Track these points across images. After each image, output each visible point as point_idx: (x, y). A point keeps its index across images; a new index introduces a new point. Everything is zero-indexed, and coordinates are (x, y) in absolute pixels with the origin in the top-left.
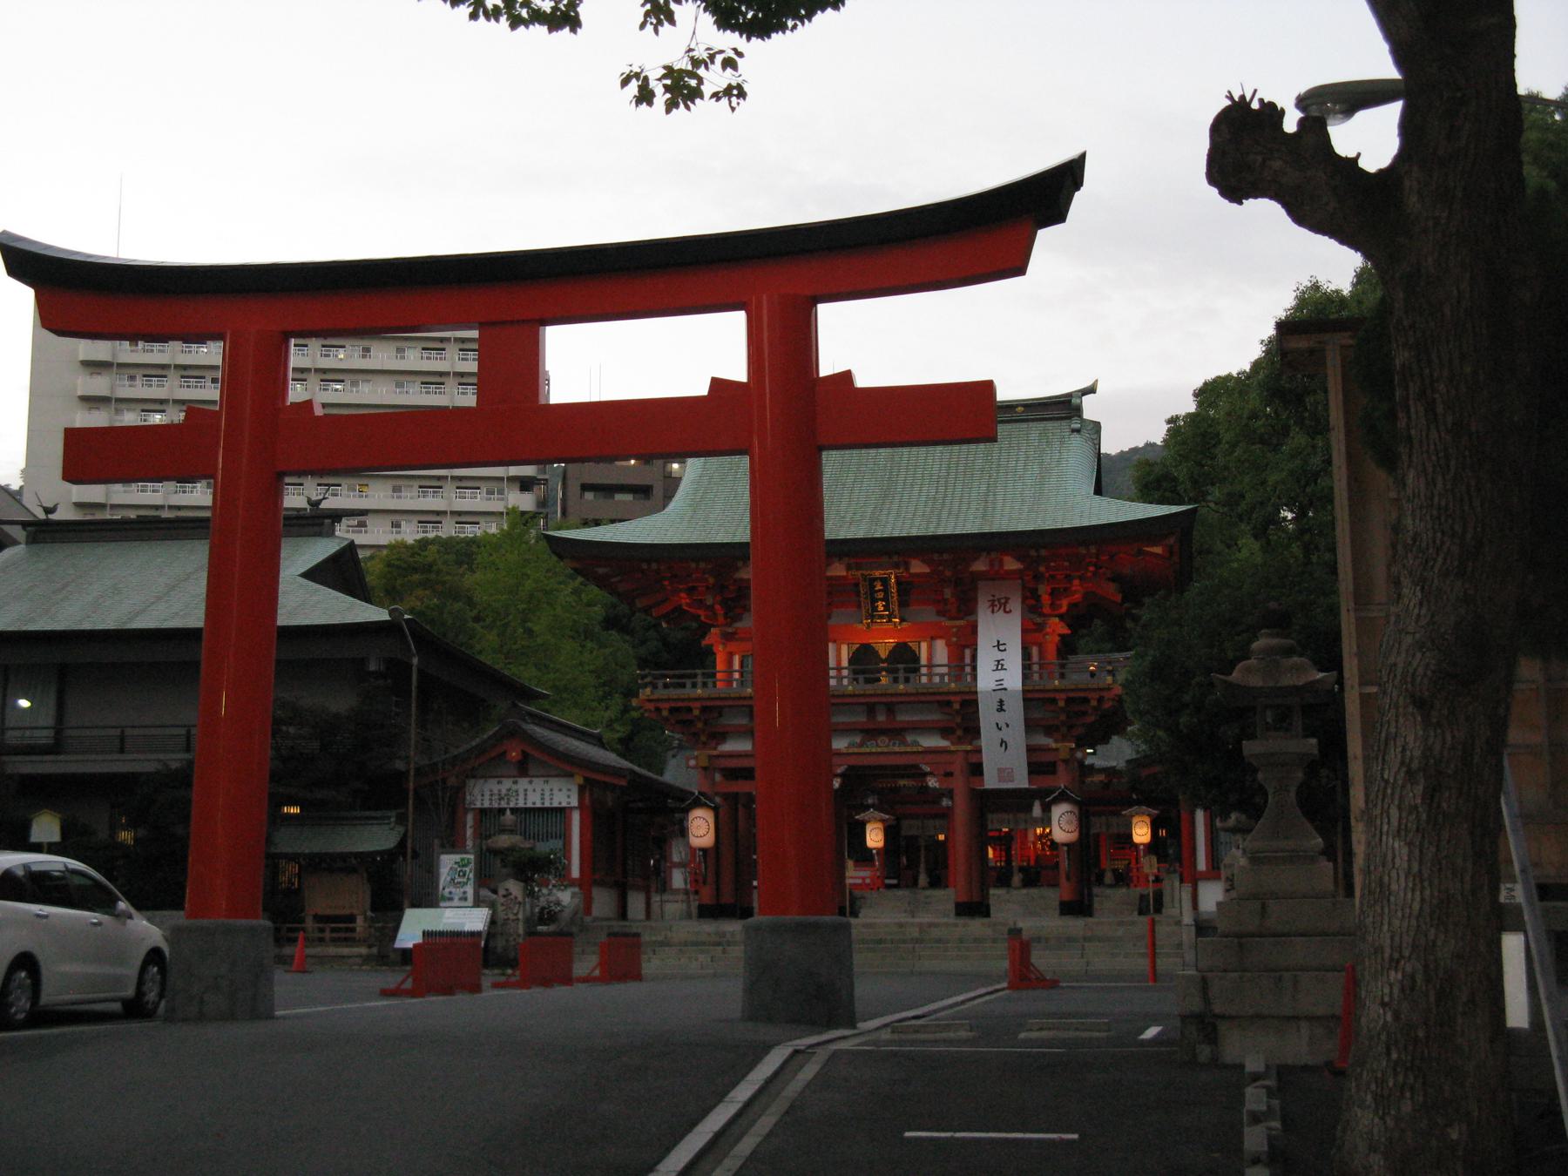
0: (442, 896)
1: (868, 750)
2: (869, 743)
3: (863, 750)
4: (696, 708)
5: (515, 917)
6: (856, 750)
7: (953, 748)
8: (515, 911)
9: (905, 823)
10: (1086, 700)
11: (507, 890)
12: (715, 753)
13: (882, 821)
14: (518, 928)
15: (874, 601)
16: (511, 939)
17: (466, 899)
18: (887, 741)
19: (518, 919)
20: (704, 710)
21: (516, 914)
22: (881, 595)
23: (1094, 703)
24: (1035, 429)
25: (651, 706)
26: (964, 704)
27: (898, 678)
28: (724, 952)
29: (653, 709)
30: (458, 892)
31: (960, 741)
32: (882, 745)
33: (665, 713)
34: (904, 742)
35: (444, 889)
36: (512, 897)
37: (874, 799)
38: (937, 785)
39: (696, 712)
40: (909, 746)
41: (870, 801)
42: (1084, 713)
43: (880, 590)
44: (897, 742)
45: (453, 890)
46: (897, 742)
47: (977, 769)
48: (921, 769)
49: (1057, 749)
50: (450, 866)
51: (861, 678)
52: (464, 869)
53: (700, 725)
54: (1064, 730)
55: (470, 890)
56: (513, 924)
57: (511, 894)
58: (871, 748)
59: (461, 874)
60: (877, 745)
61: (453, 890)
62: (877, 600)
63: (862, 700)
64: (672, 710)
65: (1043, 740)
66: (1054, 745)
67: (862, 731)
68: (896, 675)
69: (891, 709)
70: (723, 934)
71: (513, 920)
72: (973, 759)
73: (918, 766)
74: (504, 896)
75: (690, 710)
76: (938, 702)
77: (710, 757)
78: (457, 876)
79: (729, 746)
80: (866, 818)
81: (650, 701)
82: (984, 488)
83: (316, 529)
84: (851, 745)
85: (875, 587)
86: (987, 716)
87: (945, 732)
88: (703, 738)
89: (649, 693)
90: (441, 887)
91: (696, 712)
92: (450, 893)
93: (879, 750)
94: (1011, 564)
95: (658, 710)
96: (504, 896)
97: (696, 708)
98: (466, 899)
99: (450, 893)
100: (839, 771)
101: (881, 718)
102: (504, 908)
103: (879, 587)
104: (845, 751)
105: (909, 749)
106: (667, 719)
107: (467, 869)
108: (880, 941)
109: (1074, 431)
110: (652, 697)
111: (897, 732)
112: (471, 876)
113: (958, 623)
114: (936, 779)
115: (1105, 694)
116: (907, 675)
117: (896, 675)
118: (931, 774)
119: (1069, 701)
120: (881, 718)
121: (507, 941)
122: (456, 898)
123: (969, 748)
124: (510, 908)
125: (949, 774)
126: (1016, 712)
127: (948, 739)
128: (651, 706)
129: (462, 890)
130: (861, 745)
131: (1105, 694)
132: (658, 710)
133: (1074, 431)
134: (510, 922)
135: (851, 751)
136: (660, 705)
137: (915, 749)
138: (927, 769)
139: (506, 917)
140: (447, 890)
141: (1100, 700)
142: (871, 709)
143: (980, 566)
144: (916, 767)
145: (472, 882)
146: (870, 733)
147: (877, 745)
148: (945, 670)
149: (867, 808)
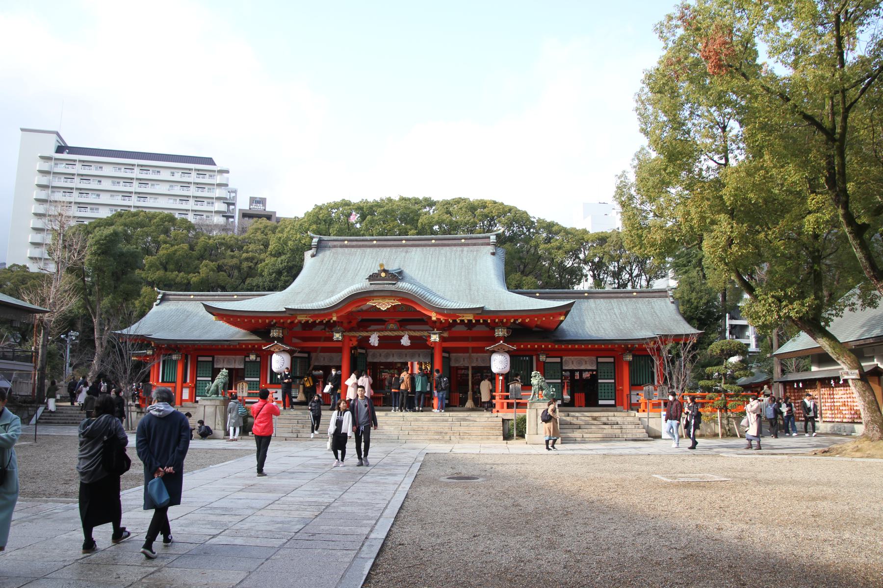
9: (313, 355)
13: (290, 352)
37: (279, 333)
80: (272, 349)
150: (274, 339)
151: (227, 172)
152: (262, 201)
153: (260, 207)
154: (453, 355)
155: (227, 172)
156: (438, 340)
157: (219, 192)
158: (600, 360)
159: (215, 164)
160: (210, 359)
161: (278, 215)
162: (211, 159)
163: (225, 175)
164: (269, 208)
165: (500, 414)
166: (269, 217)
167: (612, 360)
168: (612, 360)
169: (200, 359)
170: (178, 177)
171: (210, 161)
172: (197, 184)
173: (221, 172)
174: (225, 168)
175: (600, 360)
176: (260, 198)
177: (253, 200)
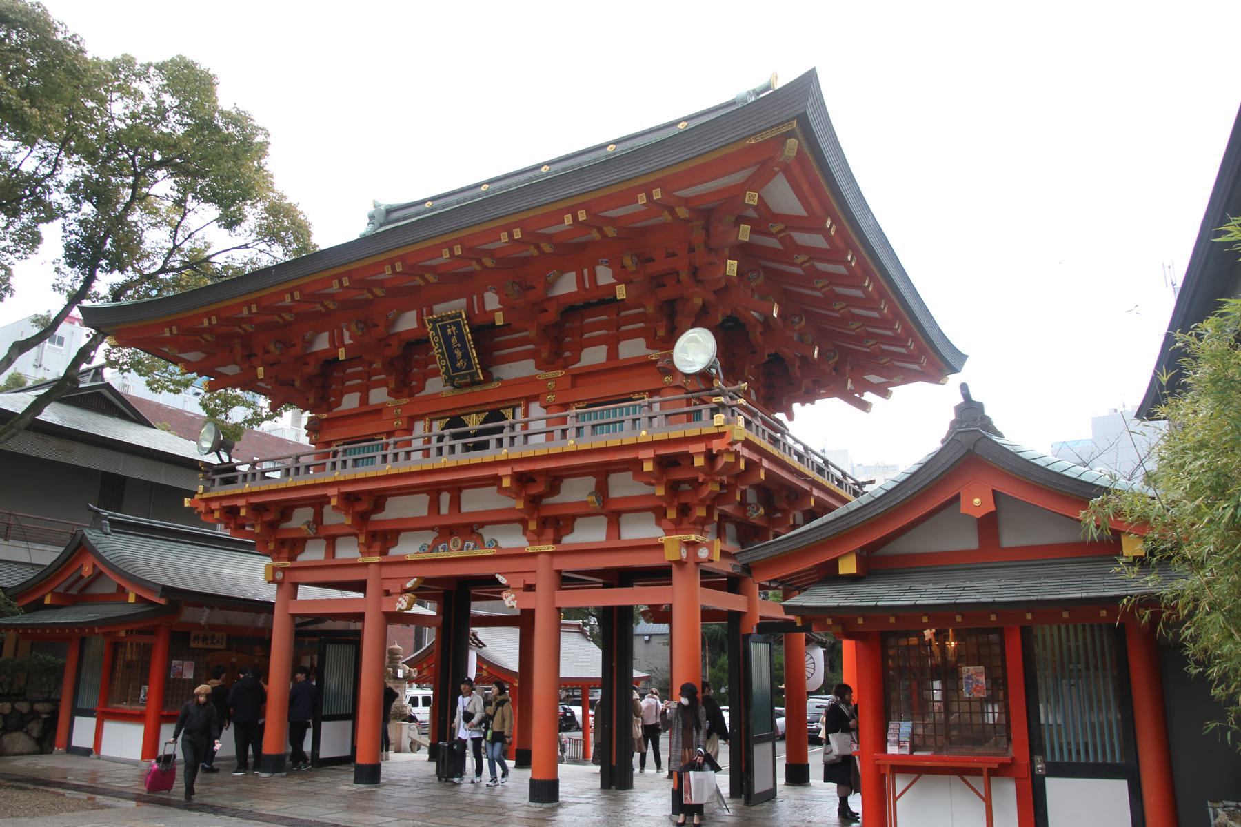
18: (460, 544)
32: (453, 549)
34: (480, 543)
38: (514, 604)
39: (243, 513)
46: (472, 545)
48: (497, 581)
67: (432, 529)
73: (494, 576)
84: (422, 549)
100: (409, 585)
111: (470, 529)
113: (559, 373)
114: (513, 596)
116: (452, 443)
125: (530, 588)
130: (433, 548)
131: (717, 445)
141: (711, 457)
146: (447, 532)
147: (450, 550)
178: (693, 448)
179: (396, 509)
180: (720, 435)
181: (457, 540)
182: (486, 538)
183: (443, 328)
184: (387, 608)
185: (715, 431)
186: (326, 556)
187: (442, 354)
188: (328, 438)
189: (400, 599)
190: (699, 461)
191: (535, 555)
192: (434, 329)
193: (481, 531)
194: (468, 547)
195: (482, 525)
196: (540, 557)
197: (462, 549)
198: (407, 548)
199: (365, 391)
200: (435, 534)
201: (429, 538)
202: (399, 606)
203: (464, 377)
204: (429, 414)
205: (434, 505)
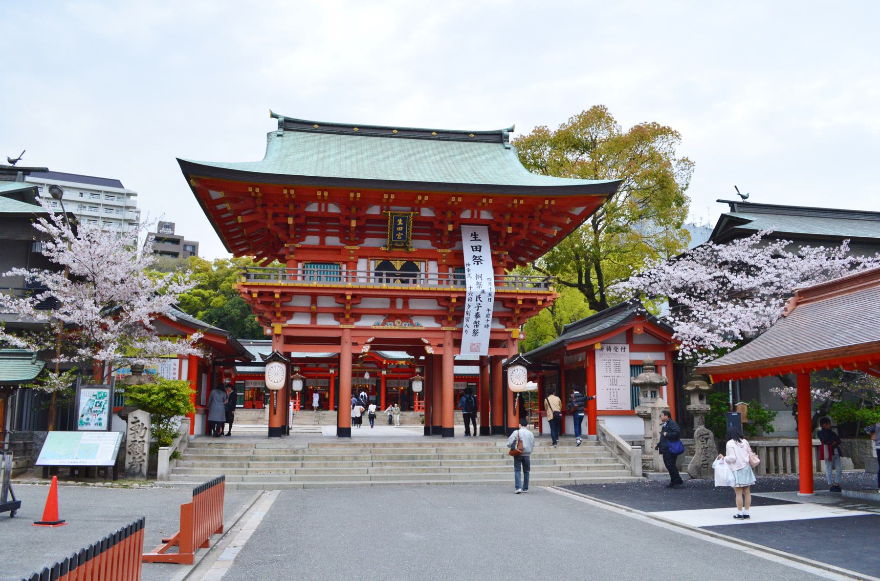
0: (81, 421)
1: (389, 327)
2: (389, 323)
3: (385, 327)
4: (277, 293)
5: (141, 440)
6: (381, 327)
7: (444, 329)
8: (142, 435)
10: (534, 301)
11: (136, 418)
12: (285, 325)
13: (302, 379)
14: (143, 449)
15: (396, 232)
16: (137, 457)
17: (100, 424)
19: (144, 441)
20: (282, 295)
21: (142, 437)
22: (400, 229)
23: (540, 303)
24: (484, 146)
25: (246, 290)
26: (458, 299)
27: (416, 280)
28: (303, 465)
29: (247, 292)
30: (94, 419)
31: (449, 324)
32: (398, 324)
33: (255, 295)
34: (412, 323)
35: (82, 416)
36: (140, 423)
38: (433, 352)
39: (277, 296)
40: (414, 326)
41: (297, 370)
42: (531, 310)
43: (401, 226)
44: (407, 324)
45: (91, 417)
47: (457, 343)
49: (510, 333)
50: (89, 398)
51: (392, 279)
52: (100, 401)
53: (278, 306)
54: (515, 320)
55: (104, 418)
56: (139, 445)
57: (138, 421)
58: (390, 326)
59: (98, 404)
60: (394, 325)
61: (91, 417)
62: (398, 232)
63: (387, 293)
64: (260, 294)
65: (499, 327)
66: (507, 330)
67: (384, 315)
68: (414, 278)
69: (406, 300)
70: (296, 452)
71: (139, 442)
72: (456, 336)
74: (133, 423)
75: (272, 294)
76: (437, 298)
77: (283, 328)
78: (94, 407)
79: (295, 321)
81: (244, 286)
82: (469, 168)
83: (13, 177)
85: (398, 223)
86: (470, 307)
87: (439, 318)
88: (278, 315)
89: (245, 281)
90: (80, 415)
91: (277, 296)
92: (88, 419)
93: (397, 328)
94: (485, 215)
95: (250, 293)
96: (133, 423)
97: (277, 293)
98: (100, 424)
99: (88, 419)
100: (369, 340)
101: (399, 305)
102: (133, 432)
103: (400, 222)
104: (374, 327)
105: (416, 328)
106: (254, 300)
107: (103, 401)
108: (413, 458)
109: (506, 148)
110: (245, 284)
111: (406, 317)
112: (107, 406)
113: (449, 251)
115: (549, 298)
117: (414, 278)
118: (429, 345)
119: (524, 301)
120: (399, 305)
121: (134, 458)
122: (92, 424)
123: (454, 329)
124: (137, 432)
125: (440, 346)
126: (488, 306)
127: (441, 323)
128: (246, 290)
129: (98, 417)
130: (383, 324)
131: (549, 298)
132: (250, 293)
133: (506, 148)
134: (137, 443)
135: (377, 327)
136: (253, 290)
137: (419, 328)
138: (426, 341)
139: (134, 439)
140: (85, 417)
141: (544, 301)
142: (393, 299)
143: (466, 215)
144: (419, 341)
145: (106, 410)
146: (391, 316)
147: (394, 325)
148: (436, 277)
149: (295, 373)
150: (295, 373)
151: (135, 195)
152: (171, 226)
153: (169, 231)
154: (388, 381)
155: (135, 195)
156: (385, 373)
157: (130, 215)
158: (469, 384)
159: (122, 187)
160: (243, 382)
161: (185, 239)
162: (119, 181)
163: (132, 198)
164: (178, 233)
165: (418, 412)
166: (176, 241)
167: (475, 384)
168: (475, 384)
169: (237, 382)
170: (86, 198)
171: (117, 183)
172: (106, 205)
173: (129, 195)
174: (133, 191)
175: (469, 384)
176: (169, 223)
177: (162, 225)
178: (539, 298)
179: (367, 304)
180: (550, 295)
181: (397, 322)
182: (414, 322)
183: (397, 219)
184: (356, 351)
185: (549, 293)
186: (312, 323)
187: (391, 230)
188: (300, 257)
189: (364, 347)
190: (540, 303)
191: (444, 331)
192: (392, 218)
193: (411, 318)
194: (405, 325)
195: (412, 315)
196: (448, 332)
197: (401, 326)
198: (365, 322)
199: (323, 235)
200: (385, 318)
201: (381, 320)
202: (363, 351)
203: (399, 243)
204: (370, 257)
205: (393, 303)
